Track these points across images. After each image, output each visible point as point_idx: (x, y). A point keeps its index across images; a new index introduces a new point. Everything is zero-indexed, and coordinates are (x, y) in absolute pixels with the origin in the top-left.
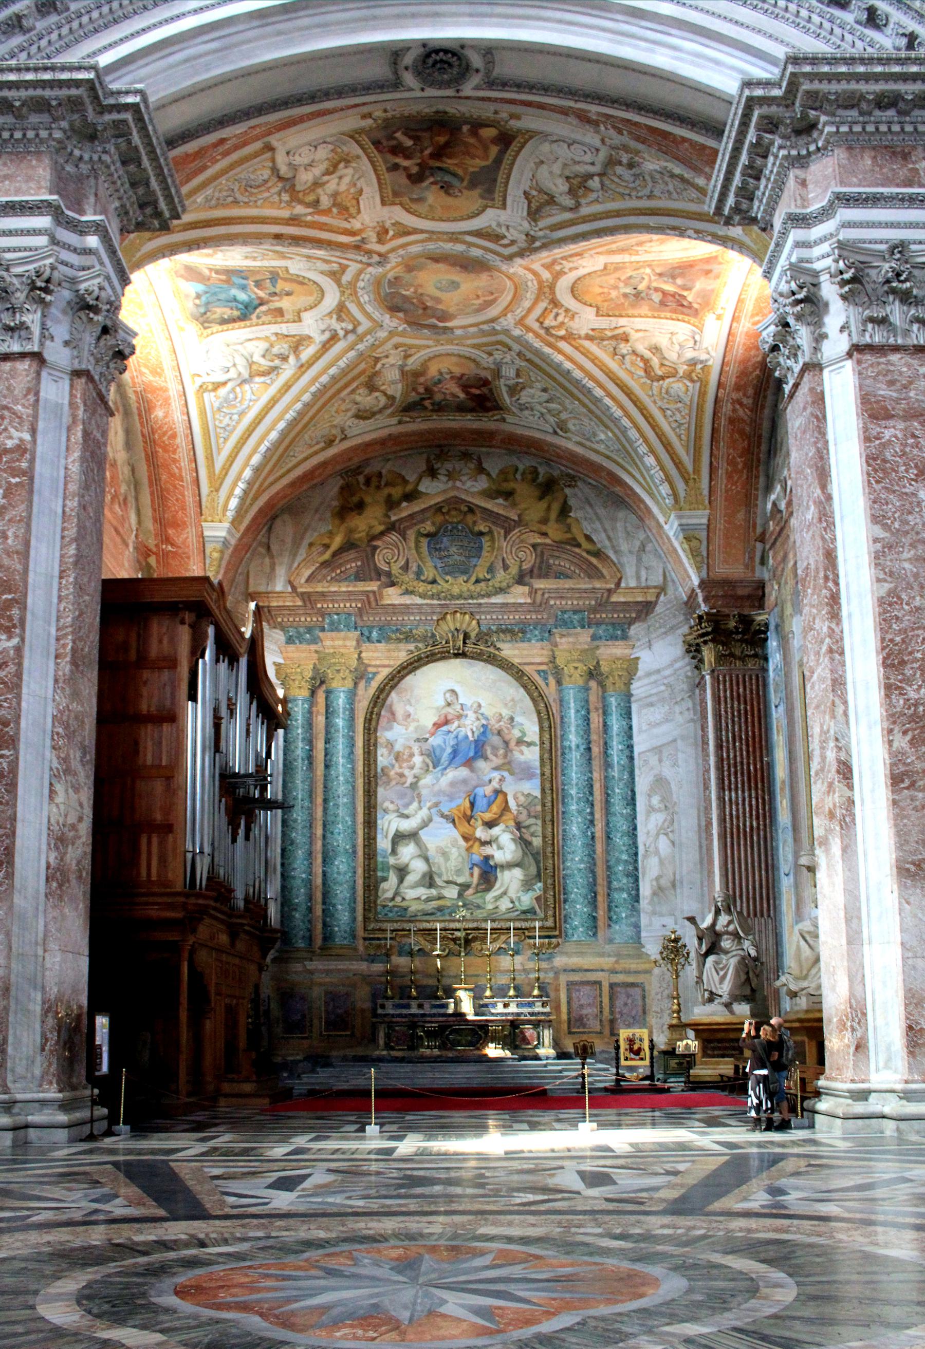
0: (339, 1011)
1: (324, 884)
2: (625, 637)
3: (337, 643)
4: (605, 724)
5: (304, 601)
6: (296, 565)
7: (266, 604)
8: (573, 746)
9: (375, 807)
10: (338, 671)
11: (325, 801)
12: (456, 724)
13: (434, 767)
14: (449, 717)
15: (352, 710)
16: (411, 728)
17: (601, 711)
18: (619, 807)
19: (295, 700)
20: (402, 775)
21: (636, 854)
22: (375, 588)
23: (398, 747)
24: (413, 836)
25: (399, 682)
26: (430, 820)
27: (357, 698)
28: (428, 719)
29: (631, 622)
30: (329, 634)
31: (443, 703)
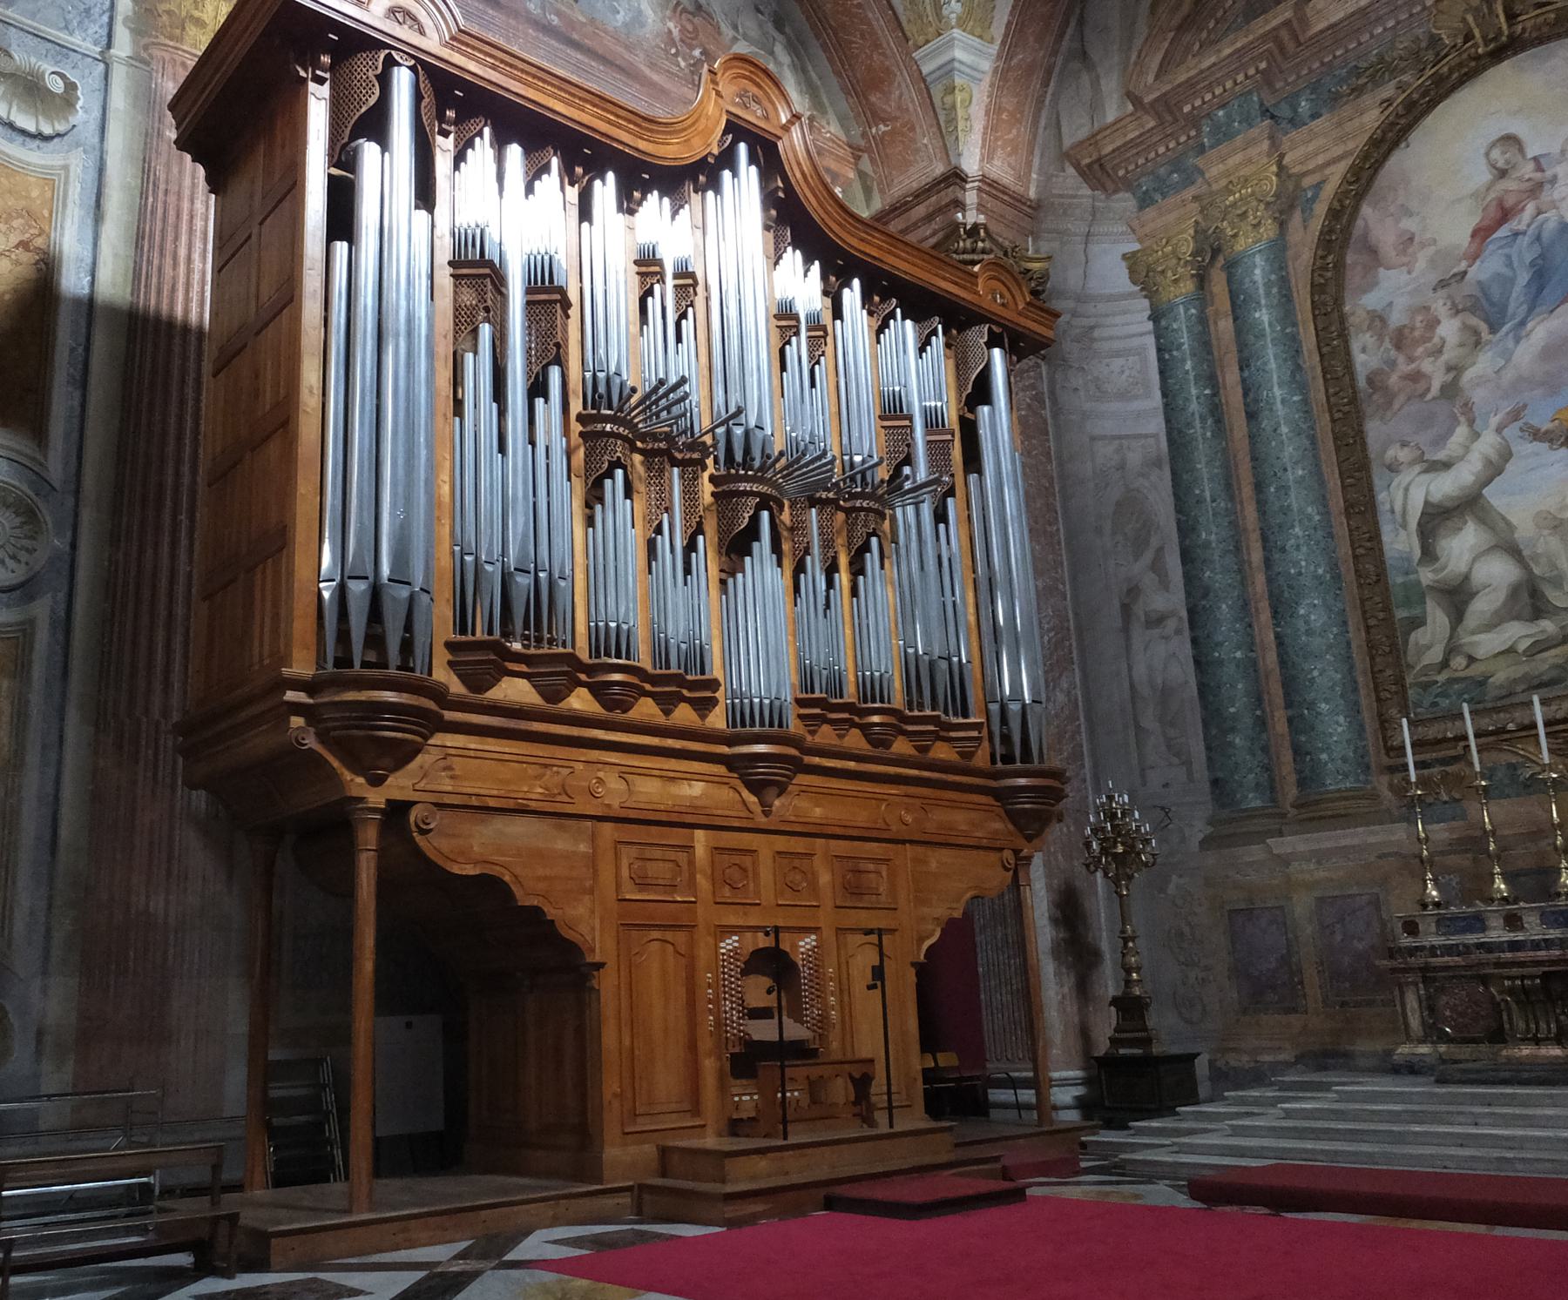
0: (1360, 946)
1: (1283, 662)
3: (1231, 162)
5: (1159, 116)
6: (1134, 57)
7: (1094, 157)
9: (1364, 466)
10: (1244, 215)
11: (1259, 487)
12: (1530, 208)
13: (1493, 329)
14: (1510, 201)
15: (1284, 282)
16: (1421, 264)
19: (1172, 307)
20: (1416, 377)
22: (1288, 14)
23: (1396, 319)
24: (1470, 505)
25: (1371, 180)
26: (1506, 455)
27: (1290, 253)
28: (1455, 229)
30: (1212, 154)
31: (1484, 176)
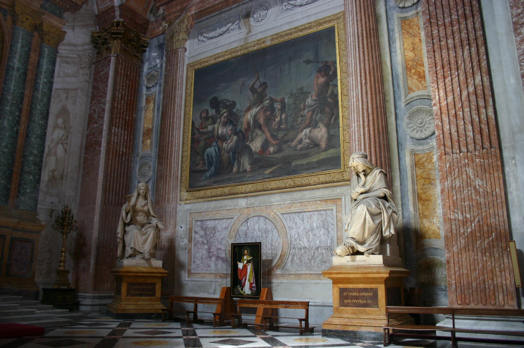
2: (61, 17)
4: (39, 62)
8: (16, 67)
17: (38, 53)
18: (37, 118)
21: (43, 152)
29: (66, 10)
